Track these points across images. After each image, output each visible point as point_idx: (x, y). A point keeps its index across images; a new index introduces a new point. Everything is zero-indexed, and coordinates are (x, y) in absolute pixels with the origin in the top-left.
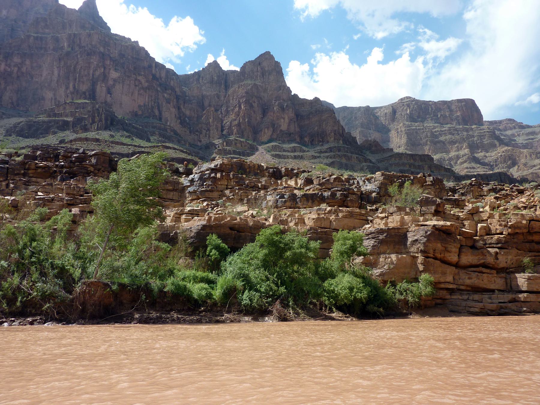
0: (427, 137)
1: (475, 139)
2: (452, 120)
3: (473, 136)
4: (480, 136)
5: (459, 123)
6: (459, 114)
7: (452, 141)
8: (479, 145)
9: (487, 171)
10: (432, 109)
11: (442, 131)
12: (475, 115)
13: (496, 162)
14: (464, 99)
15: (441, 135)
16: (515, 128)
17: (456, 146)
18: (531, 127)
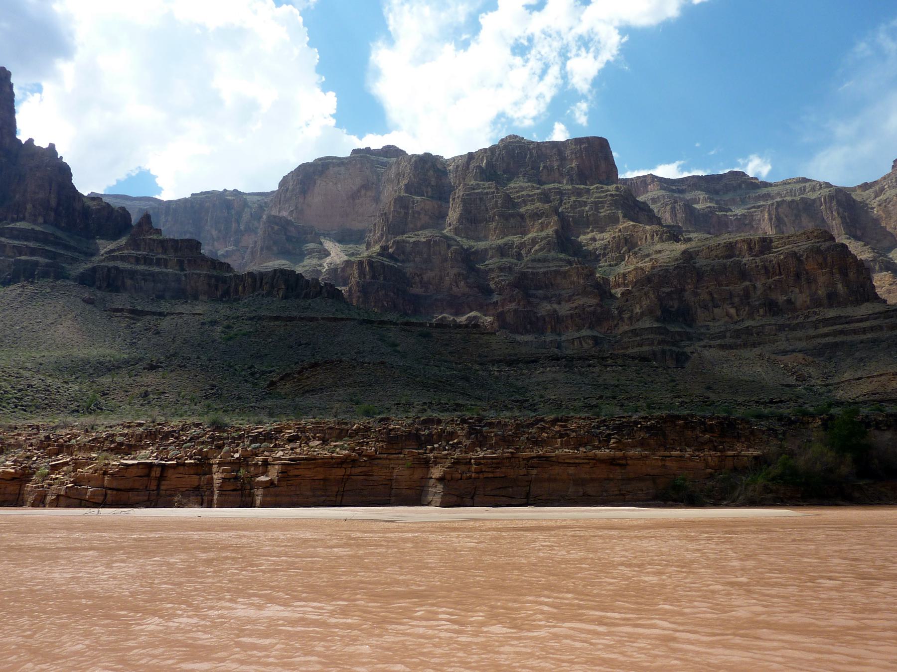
0: (497, 207)
1: (587, 208)
2: (561, 175)
3: (585, 204)
4: (596, 203)
5: (572, 180)
6: (573, 165)
7: (536, 214)
8: (591, 219)
9: (561, 266)
10: (531, 157)
11: (530, 196)
12: (603, 166)
13: (605, 249)
14: (587, 138)
15: (525, 203)
17: (540, 221)
18: (770, 185)
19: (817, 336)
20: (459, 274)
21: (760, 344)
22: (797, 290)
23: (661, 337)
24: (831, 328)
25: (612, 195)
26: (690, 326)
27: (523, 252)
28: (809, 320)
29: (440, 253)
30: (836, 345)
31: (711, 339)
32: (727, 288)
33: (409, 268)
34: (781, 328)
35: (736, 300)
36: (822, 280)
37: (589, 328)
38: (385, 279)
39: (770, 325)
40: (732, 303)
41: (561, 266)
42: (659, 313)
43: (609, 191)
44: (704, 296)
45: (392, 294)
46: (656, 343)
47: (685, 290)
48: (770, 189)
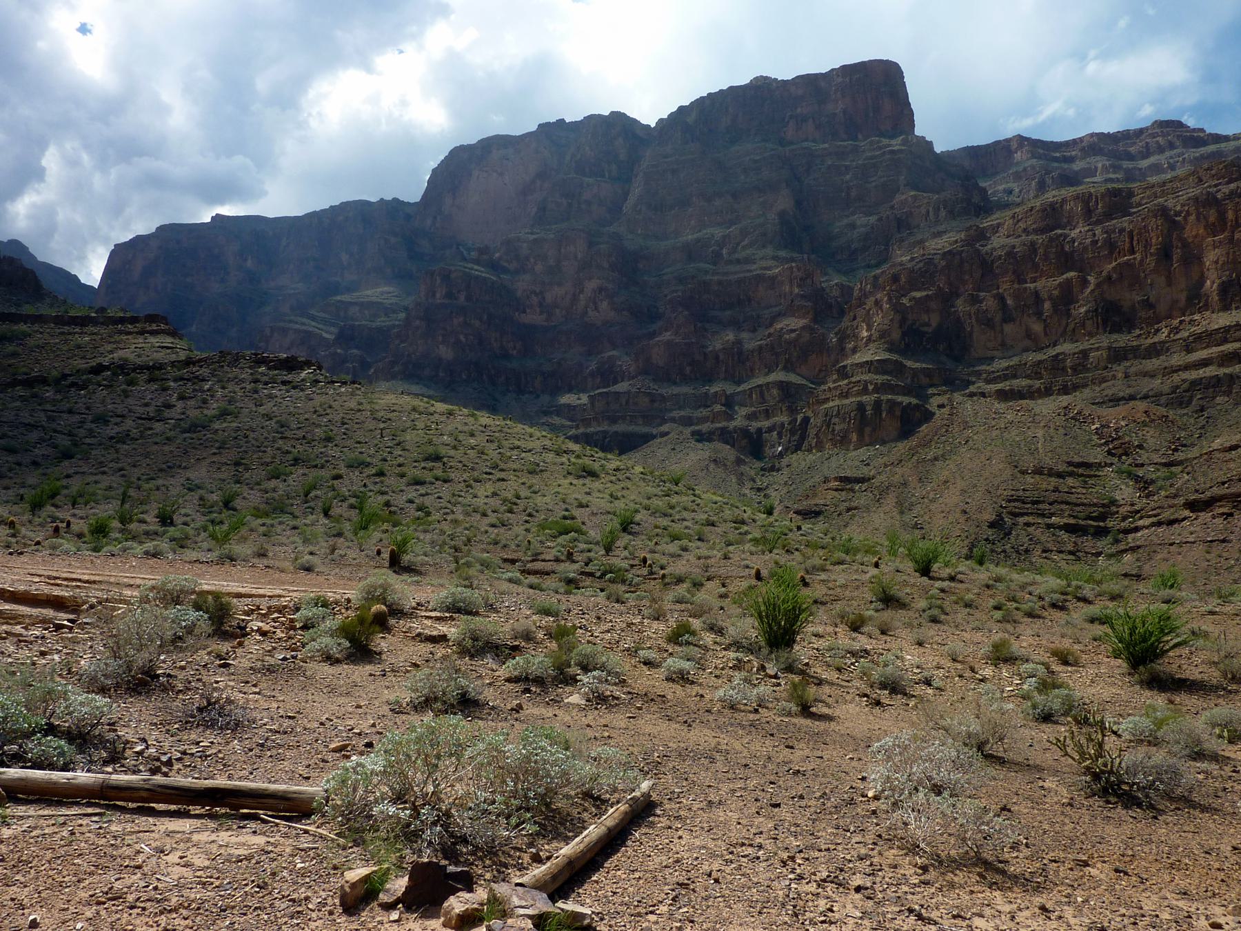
16: (1171, 146)
18: (1226, 138)
19: (1186, 368)
20: (601, 289)
21: (1076, 388)
22: (1161, 280)
23: (880, 378)
24: (1215, 349)
25: (892, 152)
26: (957, 359)
27: (724, 251)
28: (1178, 336)
29: (576, 257)
30: (1216, 382)
31: (988, 382)
32: (1032, 286)
33: (522, 285)
34: (1118, 355)
35: (1047, 305)
36: (1211, 257)
37: (785, 369)
38: (468, 298)
39: (1098, 349)
40: (1039, 314)
41: (769, 268)
42: (896, 335)
43: (890, 145)
44: (989, 303)
45: (477, 323)
46: (871, 387)
47: (958, 296)
48: (1223, 145)
